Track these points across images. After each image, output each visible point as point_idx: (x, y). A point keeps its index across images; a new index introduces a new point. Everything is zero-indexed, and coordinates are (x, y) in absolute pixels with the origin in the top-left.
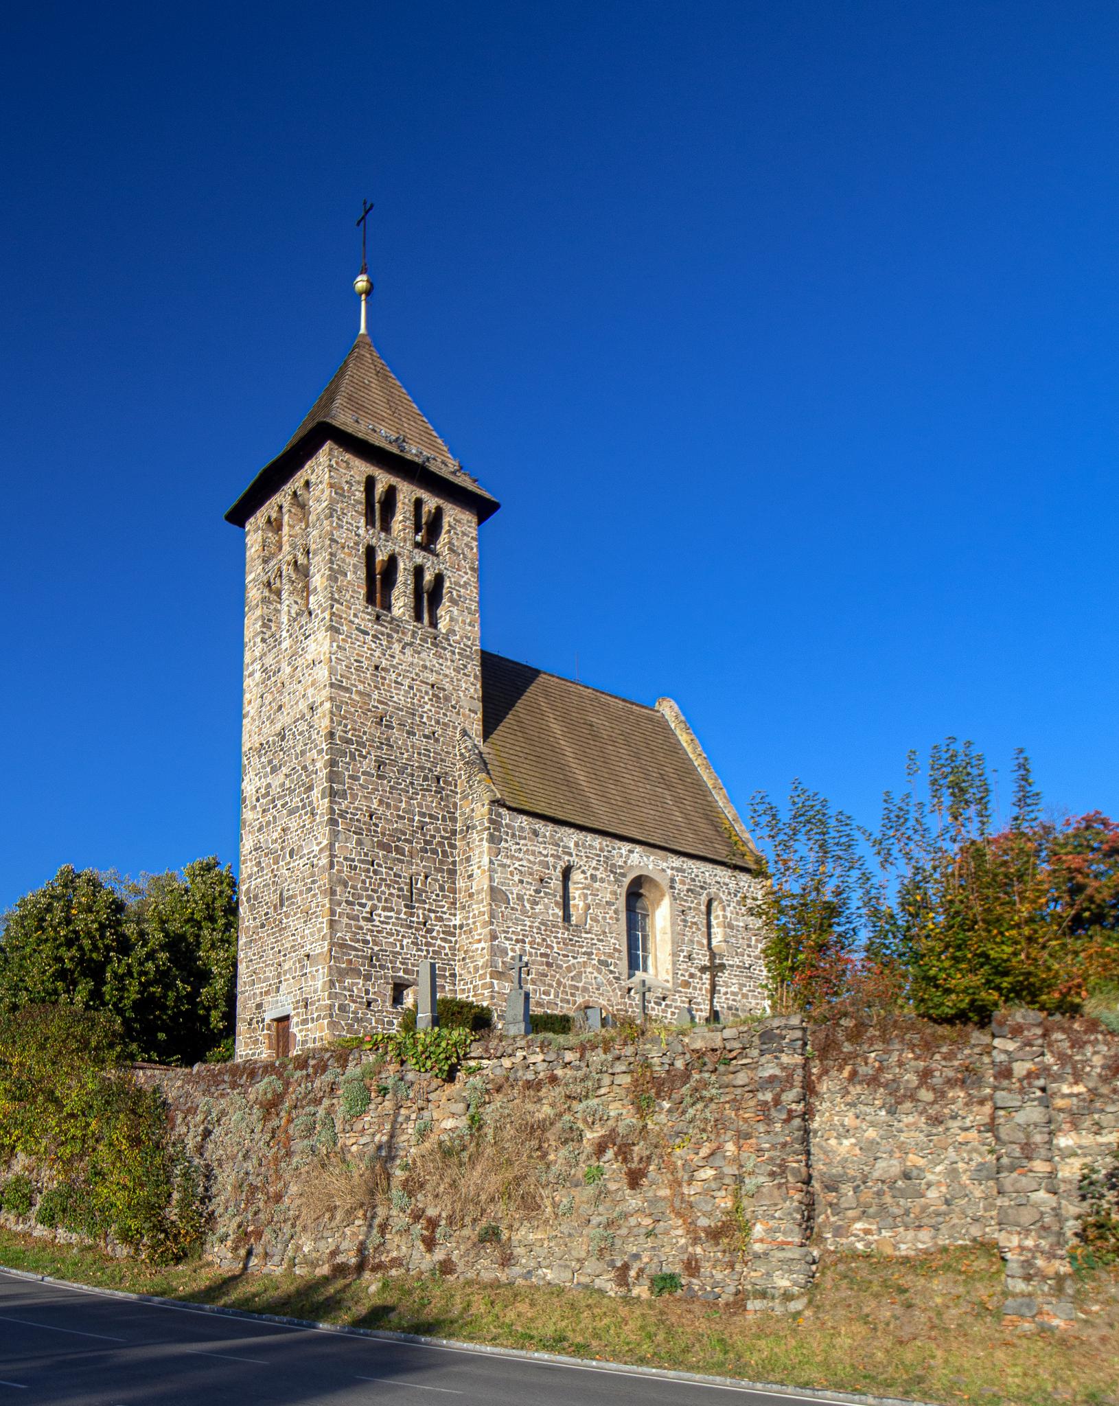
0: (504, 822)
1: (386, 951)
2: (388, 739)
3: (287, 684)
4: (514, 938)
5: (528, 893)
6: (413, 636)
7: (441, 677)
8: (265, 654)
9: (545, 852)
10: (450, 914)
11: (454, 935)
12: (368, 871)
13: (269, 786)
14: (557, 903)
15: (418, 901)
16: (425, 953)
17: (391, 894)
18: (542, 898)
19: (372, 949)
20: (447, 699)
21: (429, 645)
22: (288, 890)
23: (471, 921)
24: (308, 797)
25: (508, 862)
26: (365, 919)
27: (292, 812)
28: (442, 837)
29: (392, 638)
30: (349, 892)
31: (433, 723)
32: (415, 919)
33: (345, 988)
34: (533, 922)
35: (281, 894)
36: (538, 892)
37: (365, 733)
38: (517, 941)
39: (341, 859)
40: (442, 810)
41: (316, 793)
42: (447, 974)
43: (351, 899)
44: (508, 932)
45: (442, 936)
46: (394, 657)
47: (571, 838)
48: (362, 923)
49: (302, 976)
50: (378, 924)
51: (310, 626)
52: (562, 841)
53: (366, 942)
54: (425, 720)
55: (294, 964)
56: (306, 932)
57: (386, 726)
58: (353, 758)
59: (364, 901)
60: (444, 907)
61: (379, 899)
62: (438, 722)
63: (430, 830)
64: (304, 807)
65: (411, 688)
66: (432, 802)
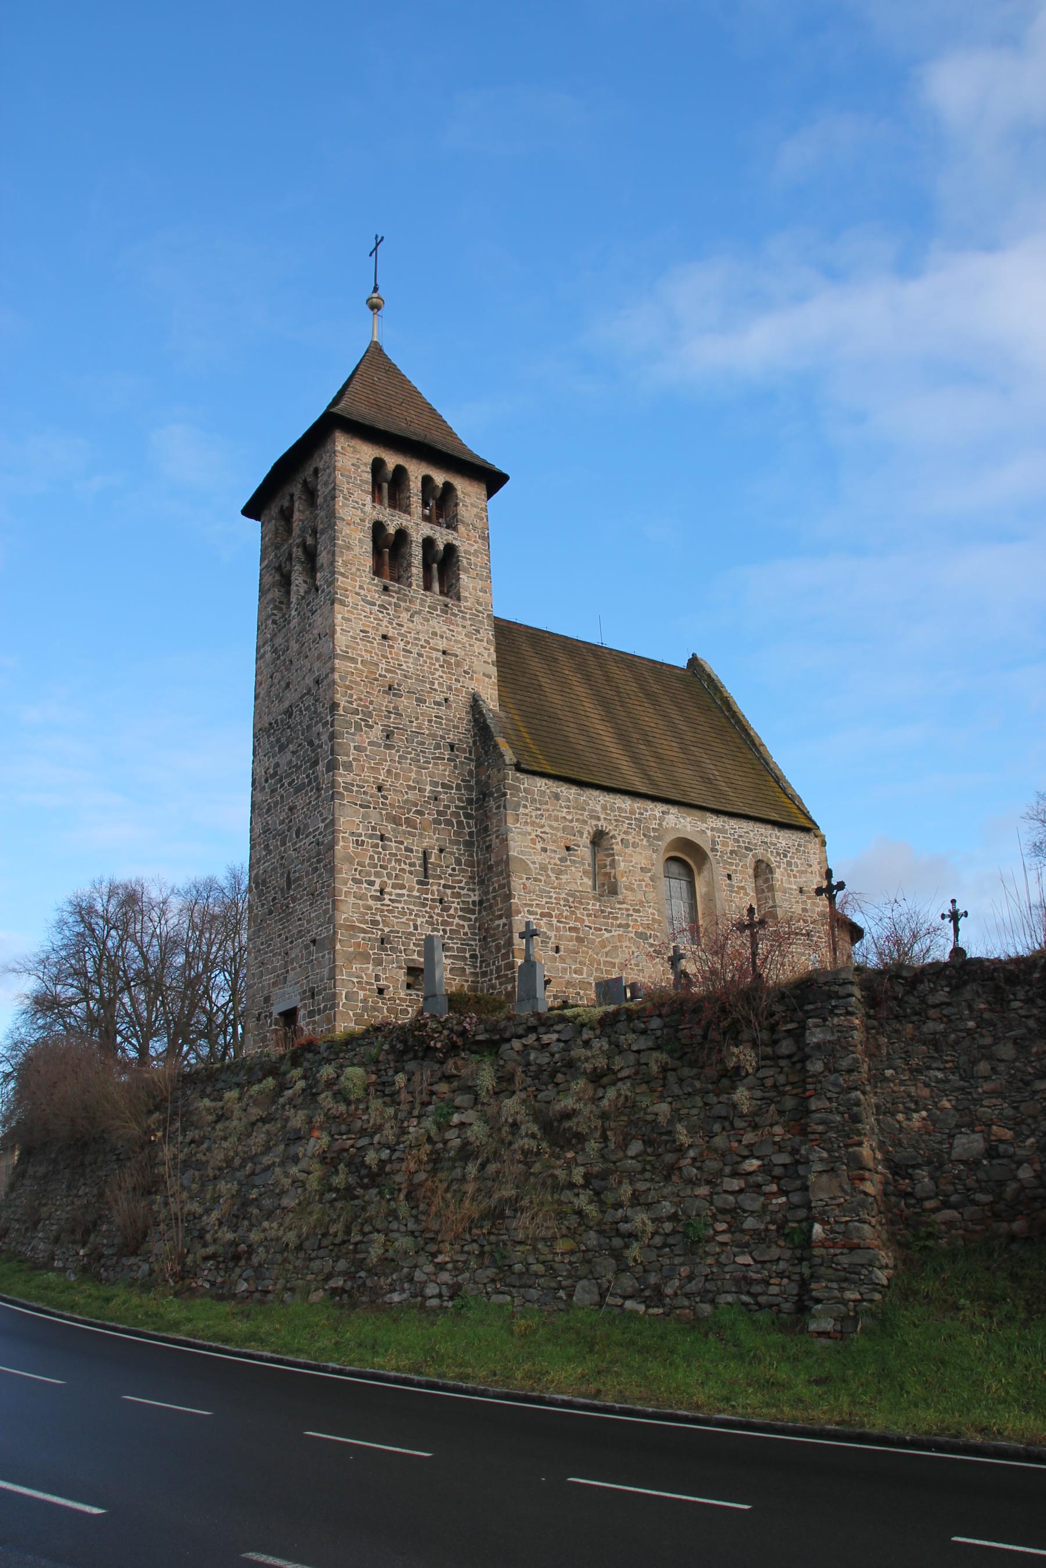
2: (396, 708)
3: (294, 660)
5: (552, 861)
6: (422, 605)
7: (452, 643)
8: (274, 636)
9: (569, 817)
11: (473, 912)
12: (376, 846)
13: (277, 765)
15: (434, 877)
16: (441, 933)
17: (402, 870)
18: (568, 866)
20: (458, 664)
21: (438, 612)
22: (295, 872)
24: (313, 773)
25: (529, 828)
27: (298, 790)
28: (457, 807)
30: (356, 870)
32: (429, 896)
35: (288, 877)
36: (563, 860)
37: (371, 702)
38: (543, 915)
40: (458, 778)
42: (467, 955)
43: (358, 876)
45: (460, 913)
46: (402, 626)
47: (597, 800)
50: (389, 903)
53: (375, 923)
54: (436, 686)
55: (301, 952)
56: (313, 915)
59: (372, 878)
60: (461, 882)
61: (389, 876)
62: (450, 688)
63: (444, 800)
64: (310, 783)
65: (420, 655)
66: (445, 770)
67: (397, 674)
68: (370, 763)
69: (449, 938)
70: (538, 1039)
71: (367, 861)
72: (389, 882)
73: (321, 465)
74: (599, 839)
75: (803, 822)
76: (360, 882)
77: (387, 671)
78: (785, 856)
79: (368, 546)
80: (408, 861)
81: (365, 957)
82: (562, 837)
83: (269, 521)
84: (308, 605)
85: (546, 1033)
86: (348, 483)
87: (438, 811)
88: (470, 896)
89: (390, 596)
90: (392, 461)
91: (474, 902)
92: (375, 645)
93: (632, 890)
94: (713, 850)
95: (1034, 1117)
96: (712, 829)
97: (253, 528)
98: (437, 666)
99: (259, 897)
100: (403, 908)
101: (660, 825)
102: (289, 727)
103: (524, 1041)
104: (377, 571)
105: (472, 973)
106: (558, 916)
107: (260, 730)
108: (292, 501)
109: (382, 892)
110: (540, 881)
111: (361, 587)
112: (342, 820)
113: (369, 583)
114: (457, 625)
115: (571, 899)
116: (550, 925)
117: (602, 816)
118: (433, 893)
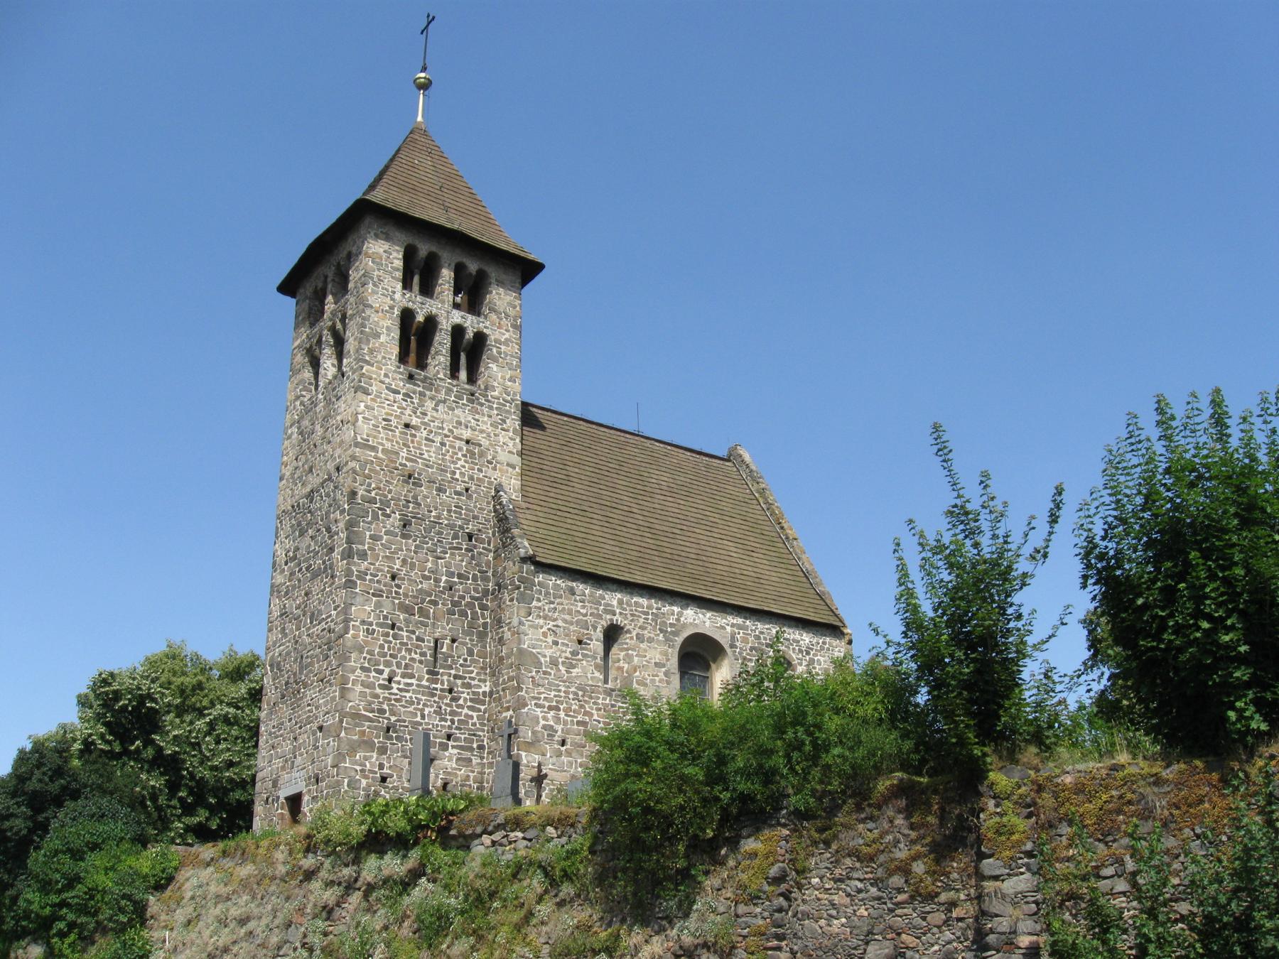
0: (536, 580)
1: (405, 721)
2: (415, 497)
4: (547, 704)
5: (563, 655)
6: (447, 394)
8: (302, 418)
9: (584, 611)
10: (480, 680)
11: (483, 703)
13: (297, 549)
14: (597, 666)
16: (449, 723)
17: (412, 660)
18: (579, 660)
19: (389, 719)
20: (482, 454)
21: (465, 402)
22: (307, 657)
23: (500, 688)
24: (329, 560)
25: (541, 621)
26: (382, 687)
27: (315, 576)
28: (472, 598)
29: (425, 396)
30: (365, 658)
31: (466, 479)
32: (439, 686)
33: (356, 763)
34: (568, 687)
36: (574, 653)
37: (390, 491)
38: (550, 708)
39: (357, 623)
41: (336, 555)
42: (475, 746)
43: (366, 665)
44: (539, 699)
45: (469, 704)
46: (426, 415)
48: (378, 691)
50: (396, 691)
51: (342, 387)
52: (604, 599)
53: (382, 711)
54: (457, 476)
56: (321, 701)
57: (414, 483)
58: (376, 517)
59: (381, 667)
60: (472, 672)
62: (471, 478)
63: (459, 591)
64: (325, 568)
65: (443, 444)
66: (462, 561)
67: (418, 463)
68: (385, 552)
69: (457, 728)
70: (507, 836)
71: (377, 650)
72: (397, 671)
73: (354, 250)
74: (612, 634)
75: (832, 620)
76: (368, 670)
77: (407, 459)
78: (808, 653)
79: (396, 334)
80: (418, 651)
81: (369, 745)
82: (574, 631)
83: (304, 301)
84: (334, 390)
85: (512, 831)
86: (379, 270)
87: (452, 601)
88: (480, 687)
89: (415, 385)
90: (424, 249)
91: (484, 693)
92: (397, 434)
93: (645, 685)
94: (733, 646)
95: (939, 927)
96: (733, 625)
97: (290, 302)
98: (460, 455)
99: (274, 680)
100: (411, 697)
101: (678, 620)
102: (310, 512)
103: (492, 837)
104: (403, 358)
105: (478, 764)
106: (567, 711)
107: (284, 511)
108: (325, 282)
109: (390, 680)
110: (550, 674)
111: (386, 375)
112: (353, 608)
113: (395, 371)
114: (483, 415)
115: (580, 693)
116: (557, 719)
117: (618, 611)
118: (442, 684)
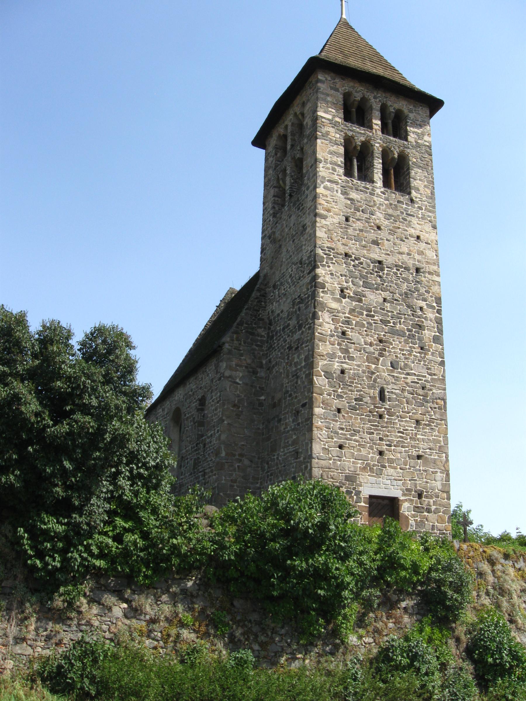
27: (393, 332)
49: (416, 470)
56: (418, 436)
102: (380, 277)
107: (333, 249)
